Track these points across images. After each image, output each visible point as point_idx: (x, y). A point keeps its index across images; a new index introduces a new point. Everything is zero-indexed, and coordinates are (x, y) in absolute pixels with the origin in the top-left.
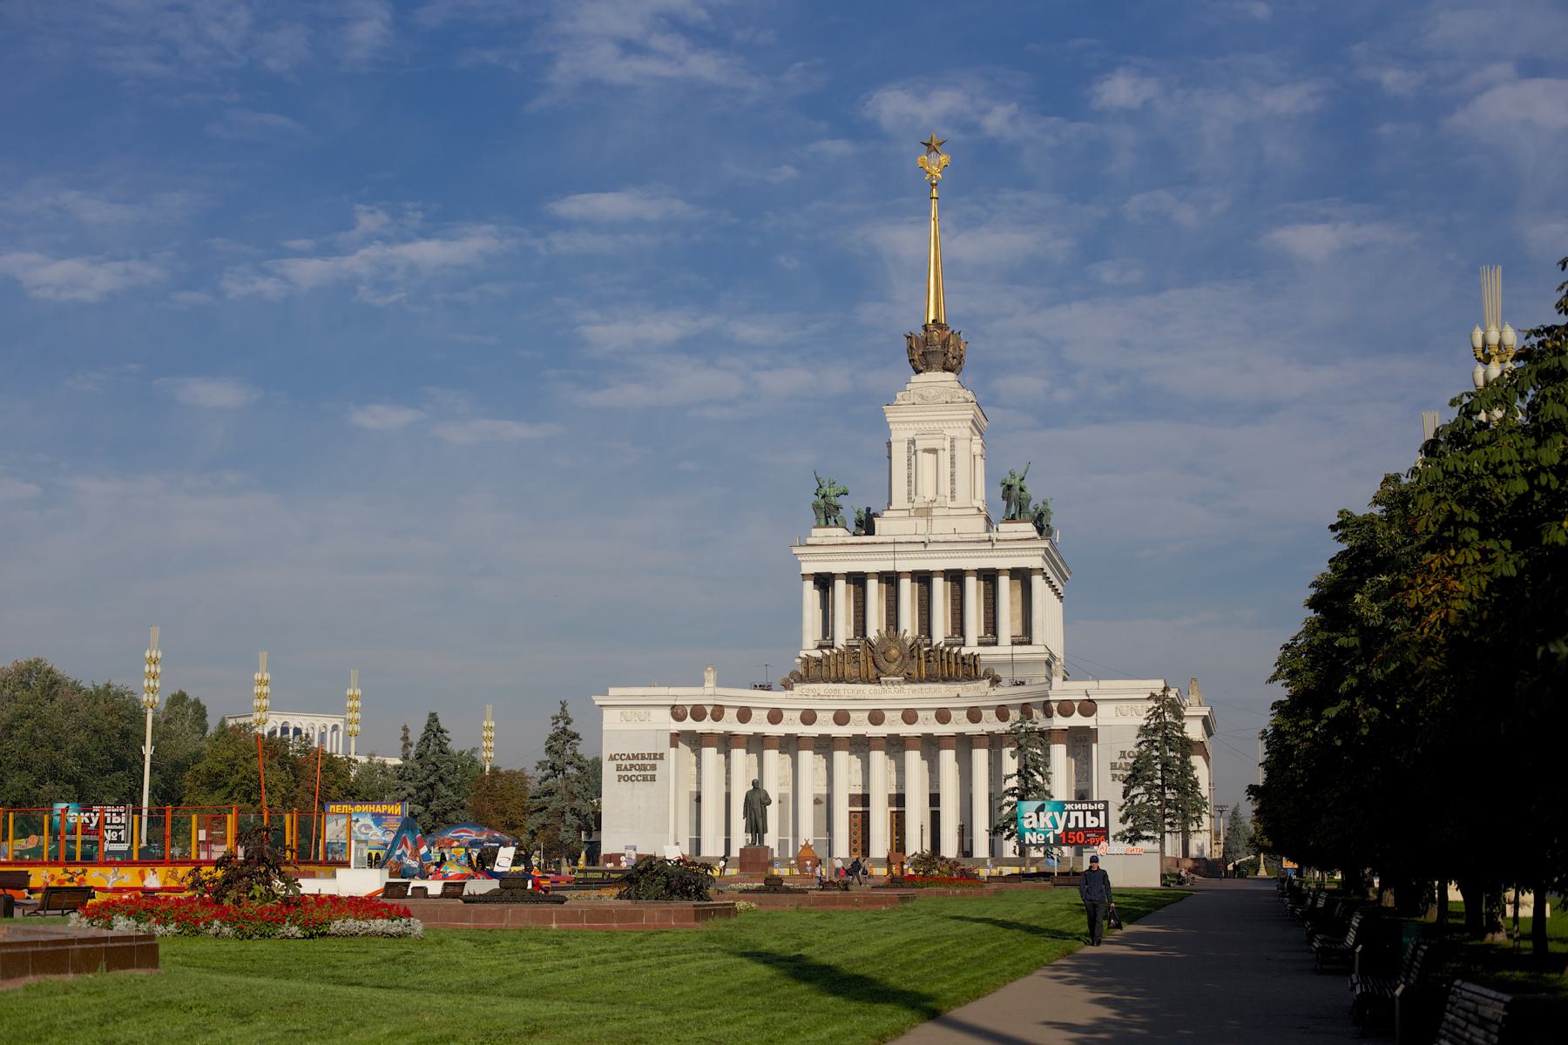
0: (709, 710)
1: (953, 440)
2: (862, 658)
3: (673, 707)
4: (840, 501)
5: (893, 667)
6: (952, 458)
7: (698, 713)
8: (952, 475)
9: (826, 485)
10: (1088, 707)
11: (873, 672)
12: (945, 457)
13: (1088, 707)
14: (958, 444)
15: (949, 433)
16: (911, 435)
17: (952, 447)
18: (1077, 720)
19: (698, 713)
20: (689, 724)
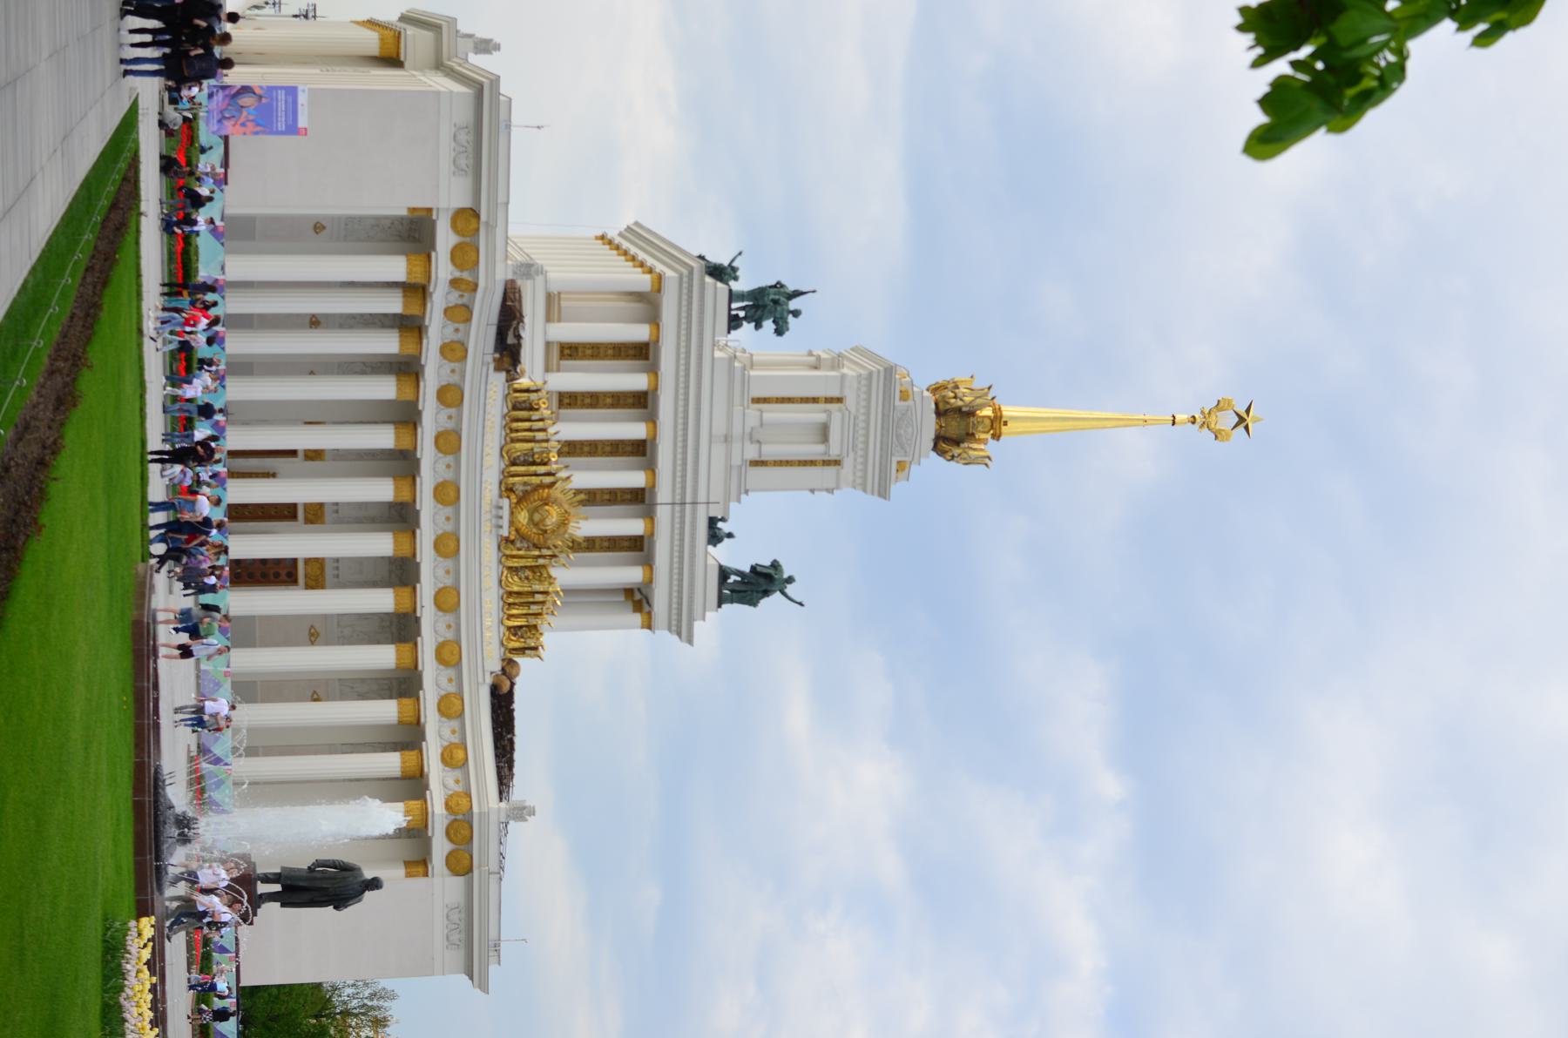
0: (466, 275)
1: (837, 463)
2: (542, 469)
3: (475, 214)
4: (769, 325)
5: (523, 517)
6: (812, 463)
7: (465, 255)
8: (788, 463)
9: (793, 304)
10: (461, 865)
11: (519, 488)
12: (815, 450)
13: (461, 865)
14: (831, 470)
15: (848, 462)
16: (850, 401)
17: (826, 463)
18: (440, 847)
19: (465, 255)
20: (445, 238)
